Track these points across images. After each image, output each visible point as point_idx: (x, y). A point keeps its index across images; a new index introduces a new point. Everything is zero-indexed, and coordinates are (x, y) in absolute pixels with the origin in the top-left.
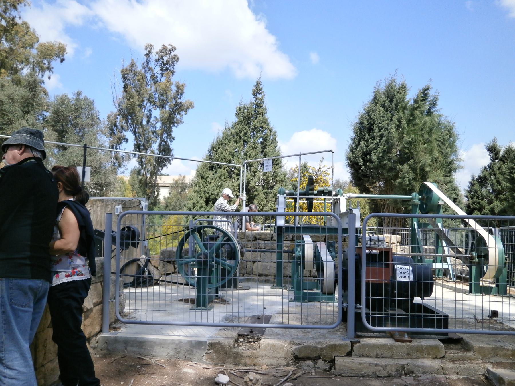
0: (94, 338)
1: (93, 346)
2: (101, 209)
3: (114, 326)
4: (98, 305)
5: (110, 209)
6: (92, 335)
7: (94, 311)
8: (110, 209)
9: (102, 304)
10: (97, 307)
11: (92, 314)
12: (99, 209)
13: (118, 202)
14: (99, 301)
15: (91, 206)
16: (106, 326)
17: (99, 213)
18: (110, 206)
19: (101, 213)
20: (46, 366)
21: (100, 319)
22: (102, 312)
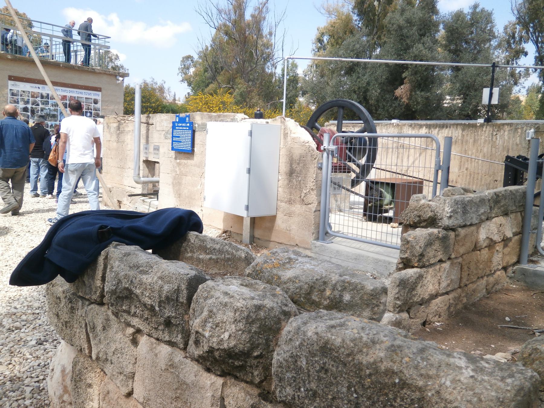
0: (511, 268)
1: (509, 275)
2: (509, 133)
3: (531, 258)
4: (517, 235)
5: (519, 134)
6: (510, 264)
7: (513, 241)
8: (519, 134)
9: (521, 235)
10: (516, 237)
11: (510, 244)
12: (506, 133)
13: (529, 125)
14: (518, 231)
15: (498, 131)
16: (525, 258)
17: (506, 138)
18: (519, 130)
19: (509, 138)
20: (469, 286)
21: (518, 250)
22: (521, 243)
